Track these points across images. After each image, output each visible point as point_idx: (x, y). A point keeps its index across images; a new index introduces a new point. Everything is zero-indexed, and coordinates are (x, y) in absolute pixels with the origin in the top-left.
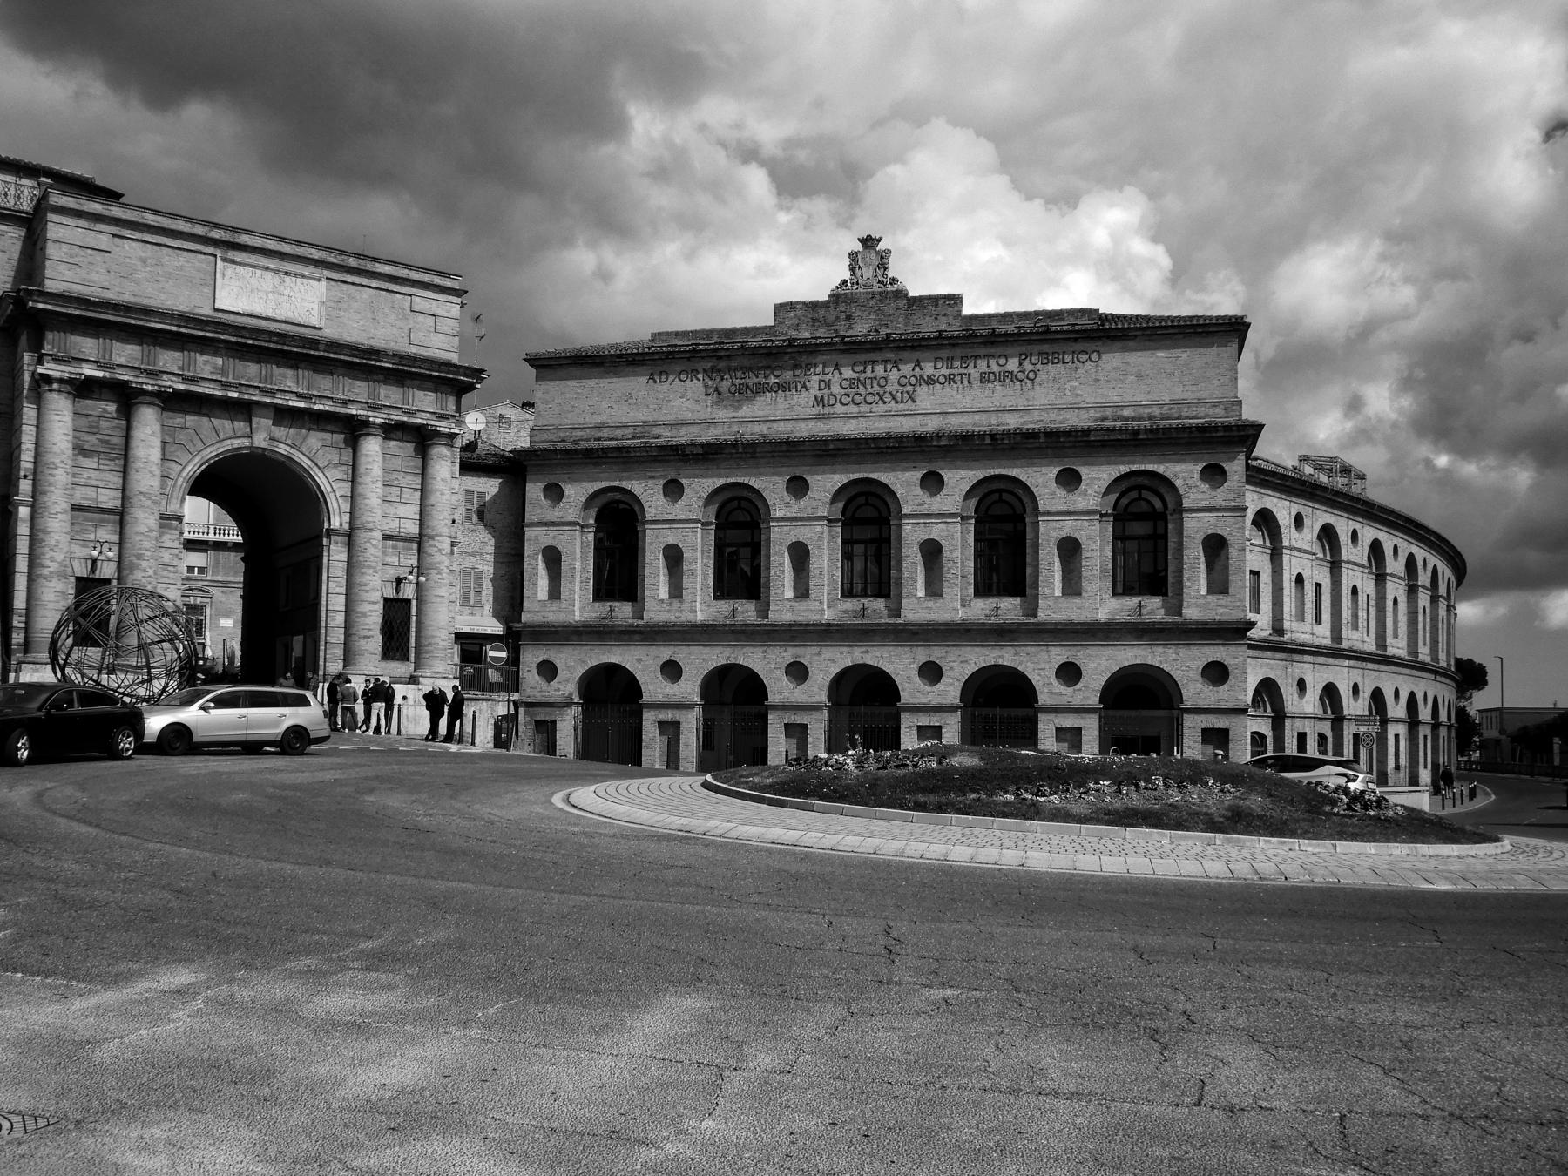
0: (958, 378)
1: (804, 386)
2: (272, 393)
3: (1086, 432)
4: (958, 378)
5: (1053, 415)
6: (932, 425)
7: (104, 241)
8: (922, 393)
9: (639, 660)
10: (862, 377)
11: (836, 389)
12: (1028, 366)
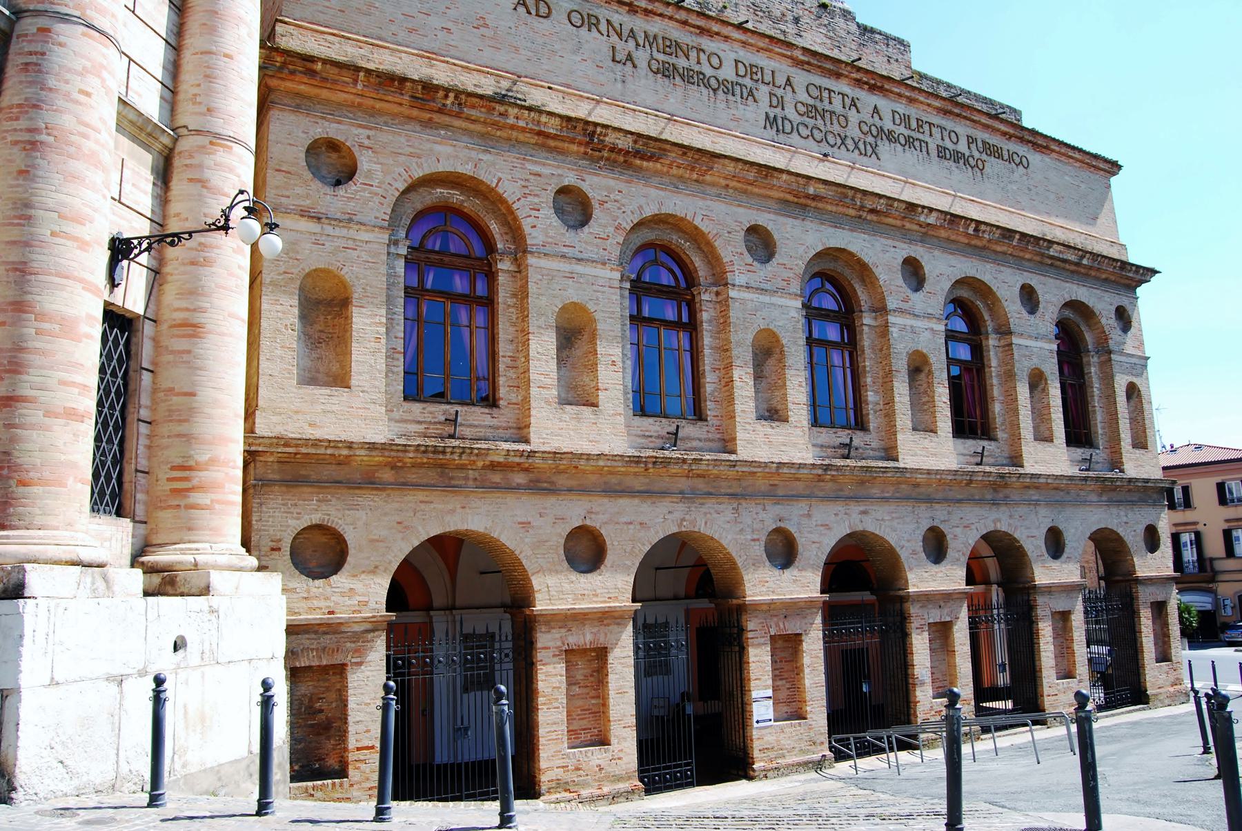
0: (917, 144)
1: (751, 93)
4: (917, 144)
10: (818, 104)
11: (790, 112)
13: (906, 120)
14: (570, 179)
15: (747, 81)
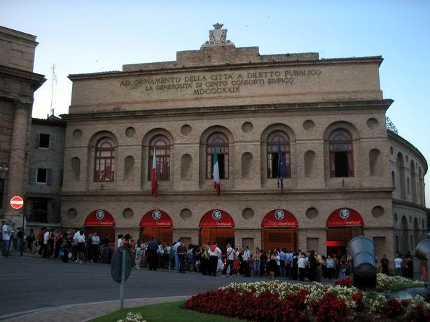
3: (316, 104)
5: (300, 97)
6: (247, 102)
8: (242, 88)
9: (114, 208)
12: (289, 77)
13: (254, 75)
14: (129, 125)
15: (189, 82)
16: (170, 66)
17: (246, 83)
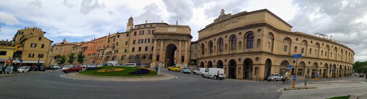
2: (172, 38)
7: (159, 28)
16: (213, 24)
17: (227, 24)
